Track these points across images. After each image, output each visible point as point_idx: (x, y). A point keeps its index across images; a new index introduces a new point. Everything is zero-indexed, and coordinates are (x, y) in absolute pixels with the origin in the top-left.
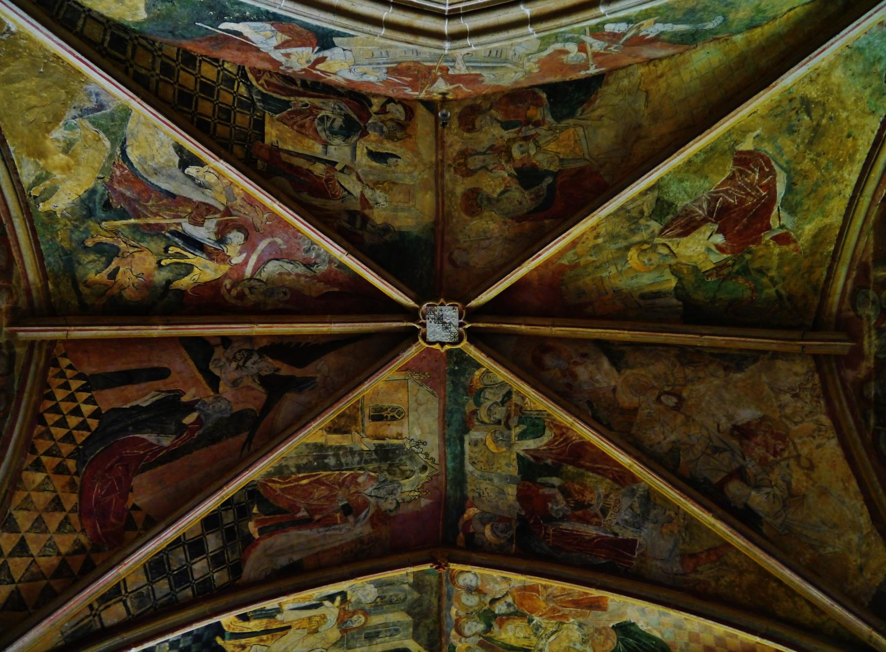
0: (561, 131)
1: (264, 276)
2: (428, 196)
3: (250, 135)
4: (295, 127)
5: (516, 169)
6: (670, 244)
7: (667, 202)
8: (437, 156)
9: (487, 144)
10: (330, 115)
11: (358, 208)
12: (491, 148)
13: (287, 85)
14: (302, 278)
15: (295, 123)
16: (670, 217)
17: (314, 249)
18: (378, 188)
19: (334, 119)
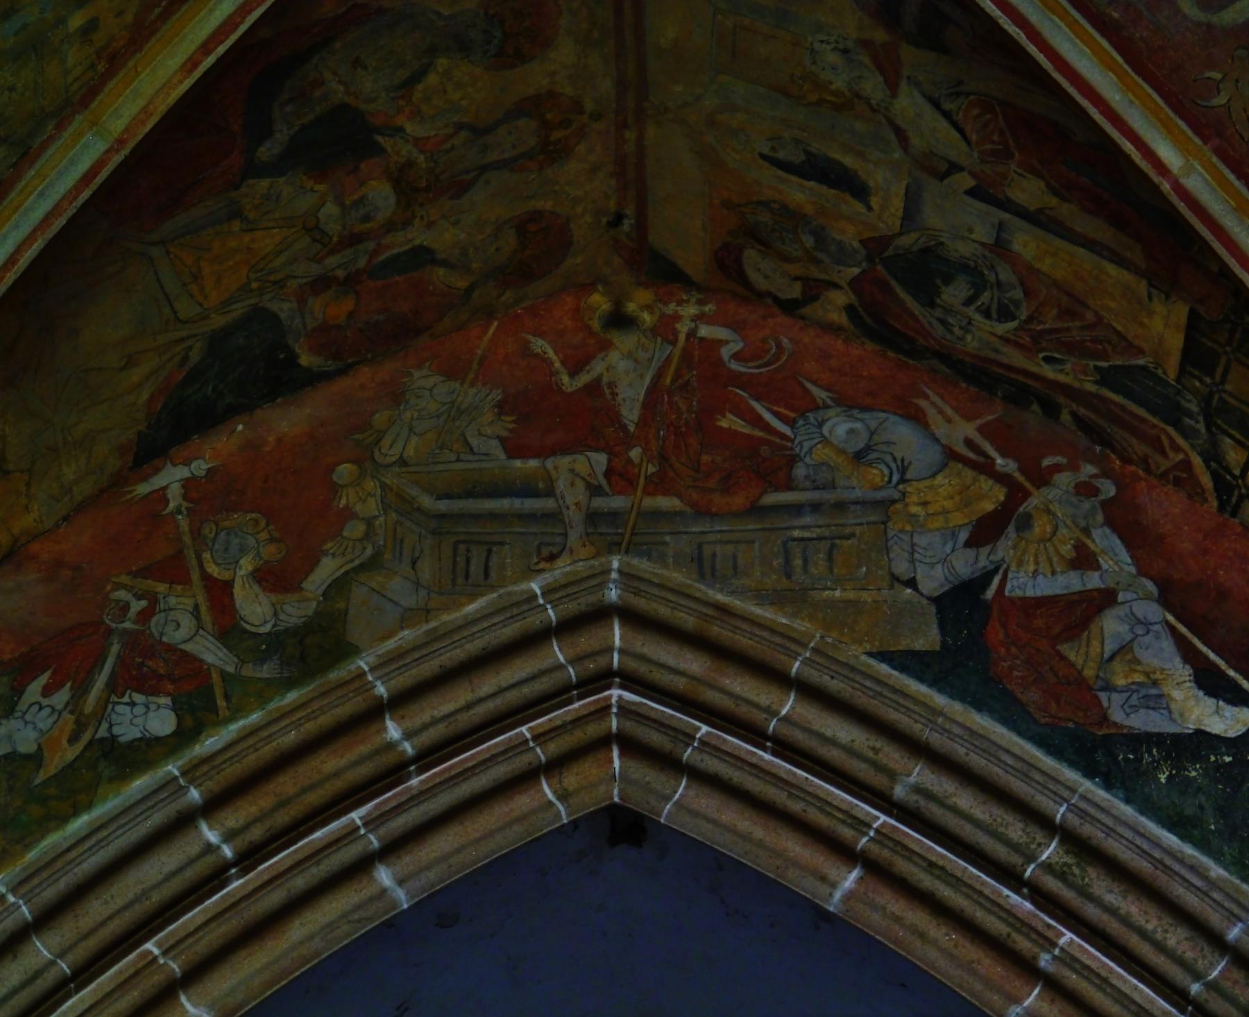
4: (1090, 316)
10: (978, 317)
11: (908, 53)
12: (460, 188)
19: (969, 302)
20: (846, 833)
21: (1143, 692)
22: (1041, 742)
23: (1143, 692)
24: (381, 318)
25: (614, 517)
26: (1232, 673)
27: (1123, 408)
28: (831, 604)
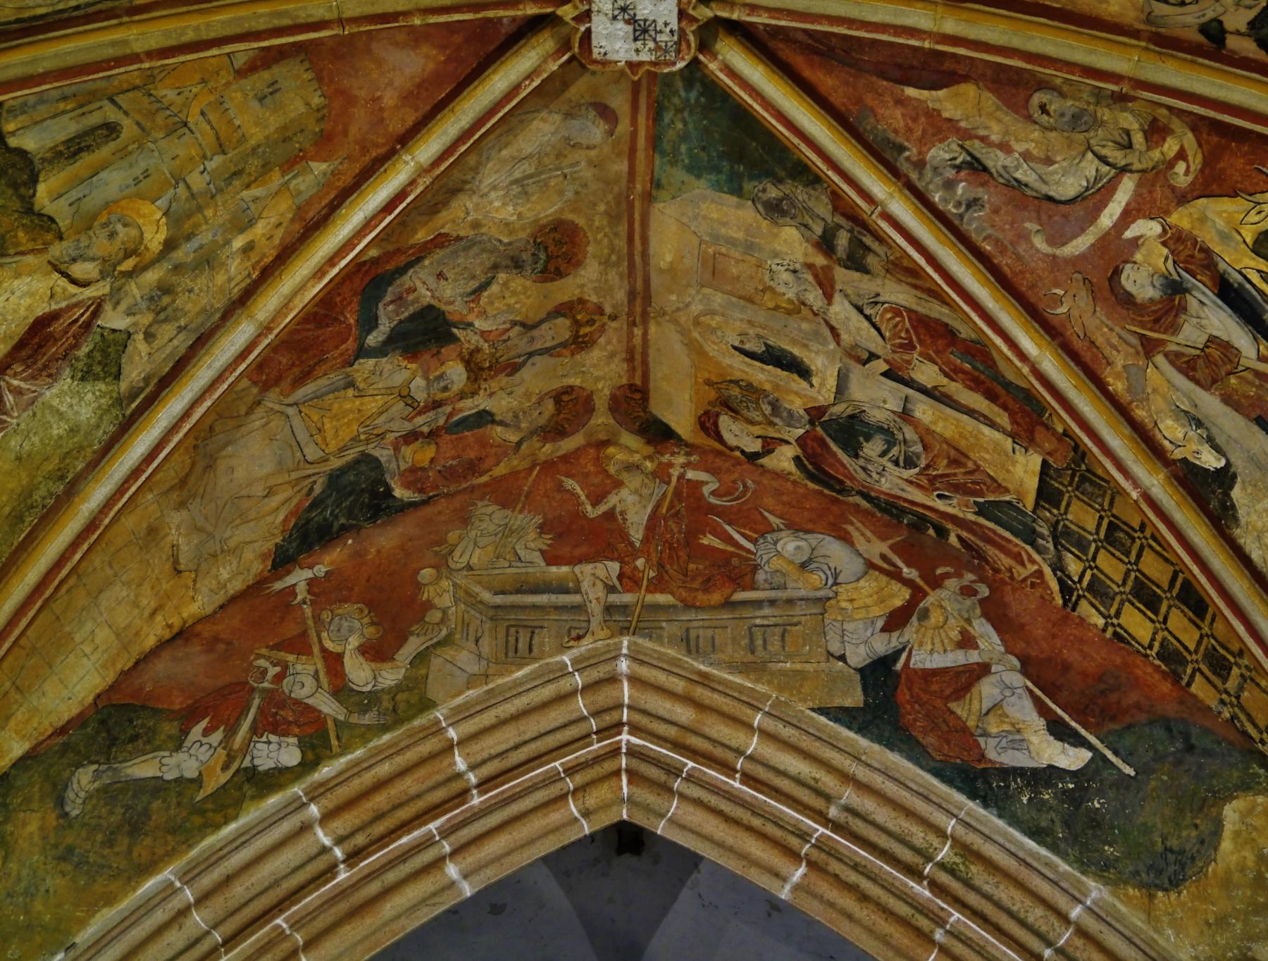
0: (355, 439)
1: (1090, 167)
2: (668, 258)
3: (1070, 484)
4: (970, 465)
5: (455, 339)
6: (73, 289)
7: (97, 378)
8: (645, 334)
9: (526, 373)
10: (889, 465)
11: (840, 274)
12: (514, 368)
13: (981, 544)
14: (995, 138)
15: (971, 473)
16: (84, 350)
17: (959, 204)
18: (790, 301)
19: (883, 454)
20: (794, 842)
21: (1010, 737)
22: (937, 774)
23: (1010, 737)
24: (454, 463)
25: (624, 608)
26: (1073, 724)
27: (994, 532)
28: (783, 673)
